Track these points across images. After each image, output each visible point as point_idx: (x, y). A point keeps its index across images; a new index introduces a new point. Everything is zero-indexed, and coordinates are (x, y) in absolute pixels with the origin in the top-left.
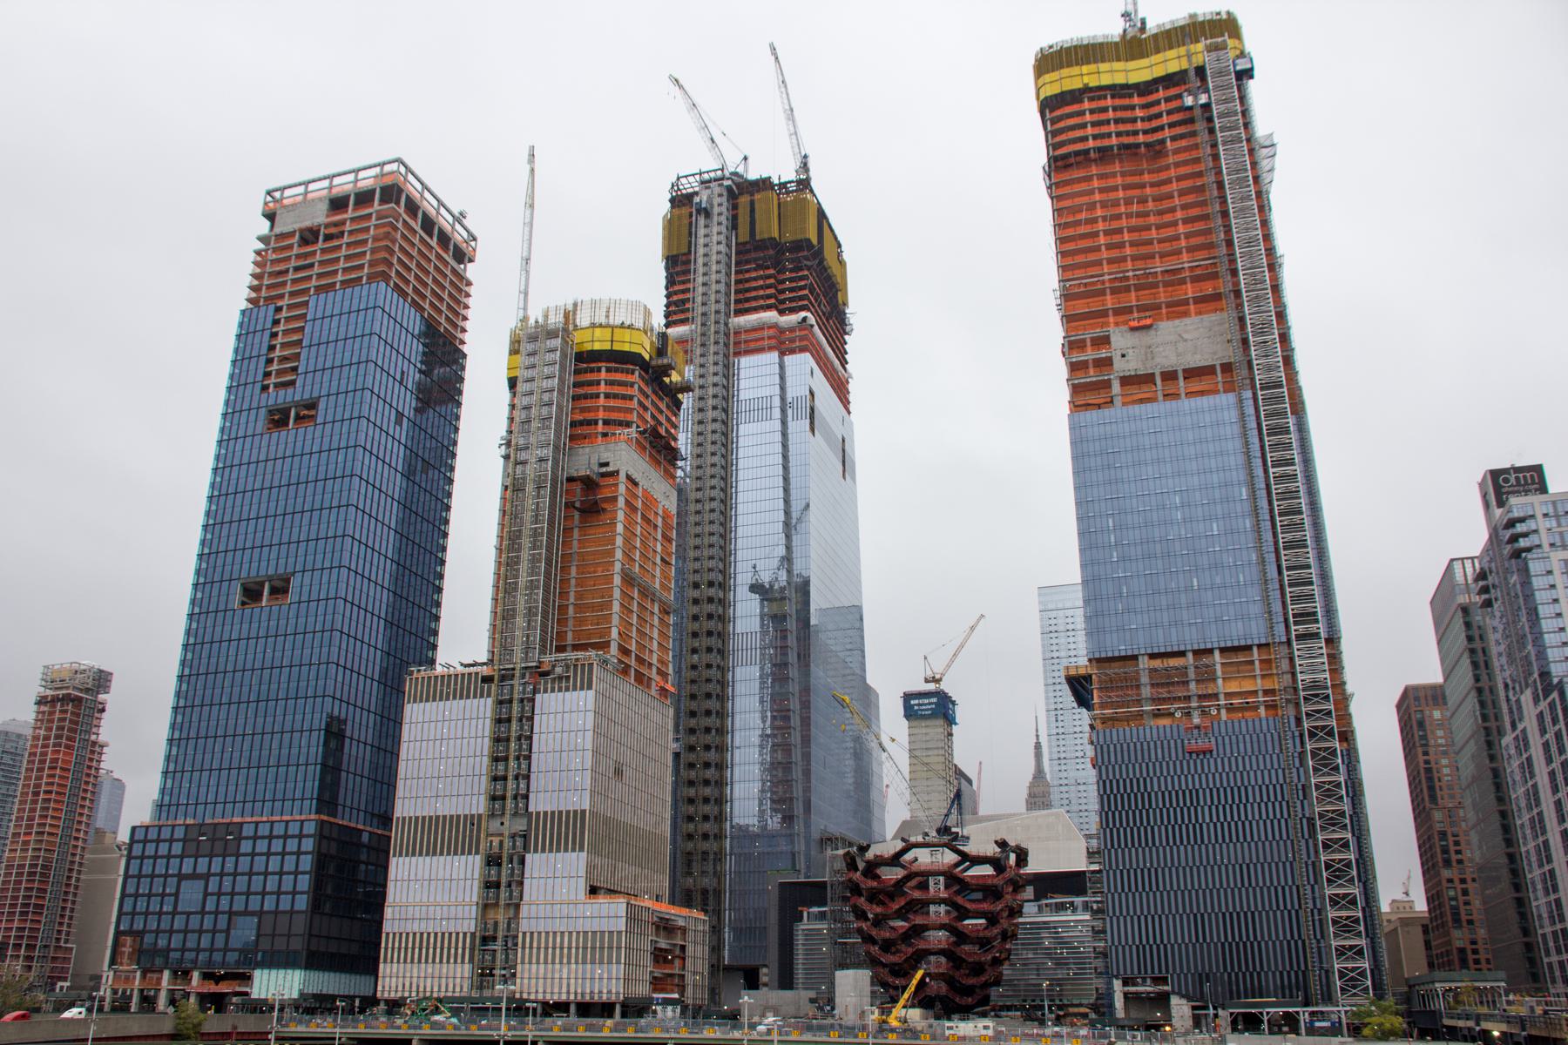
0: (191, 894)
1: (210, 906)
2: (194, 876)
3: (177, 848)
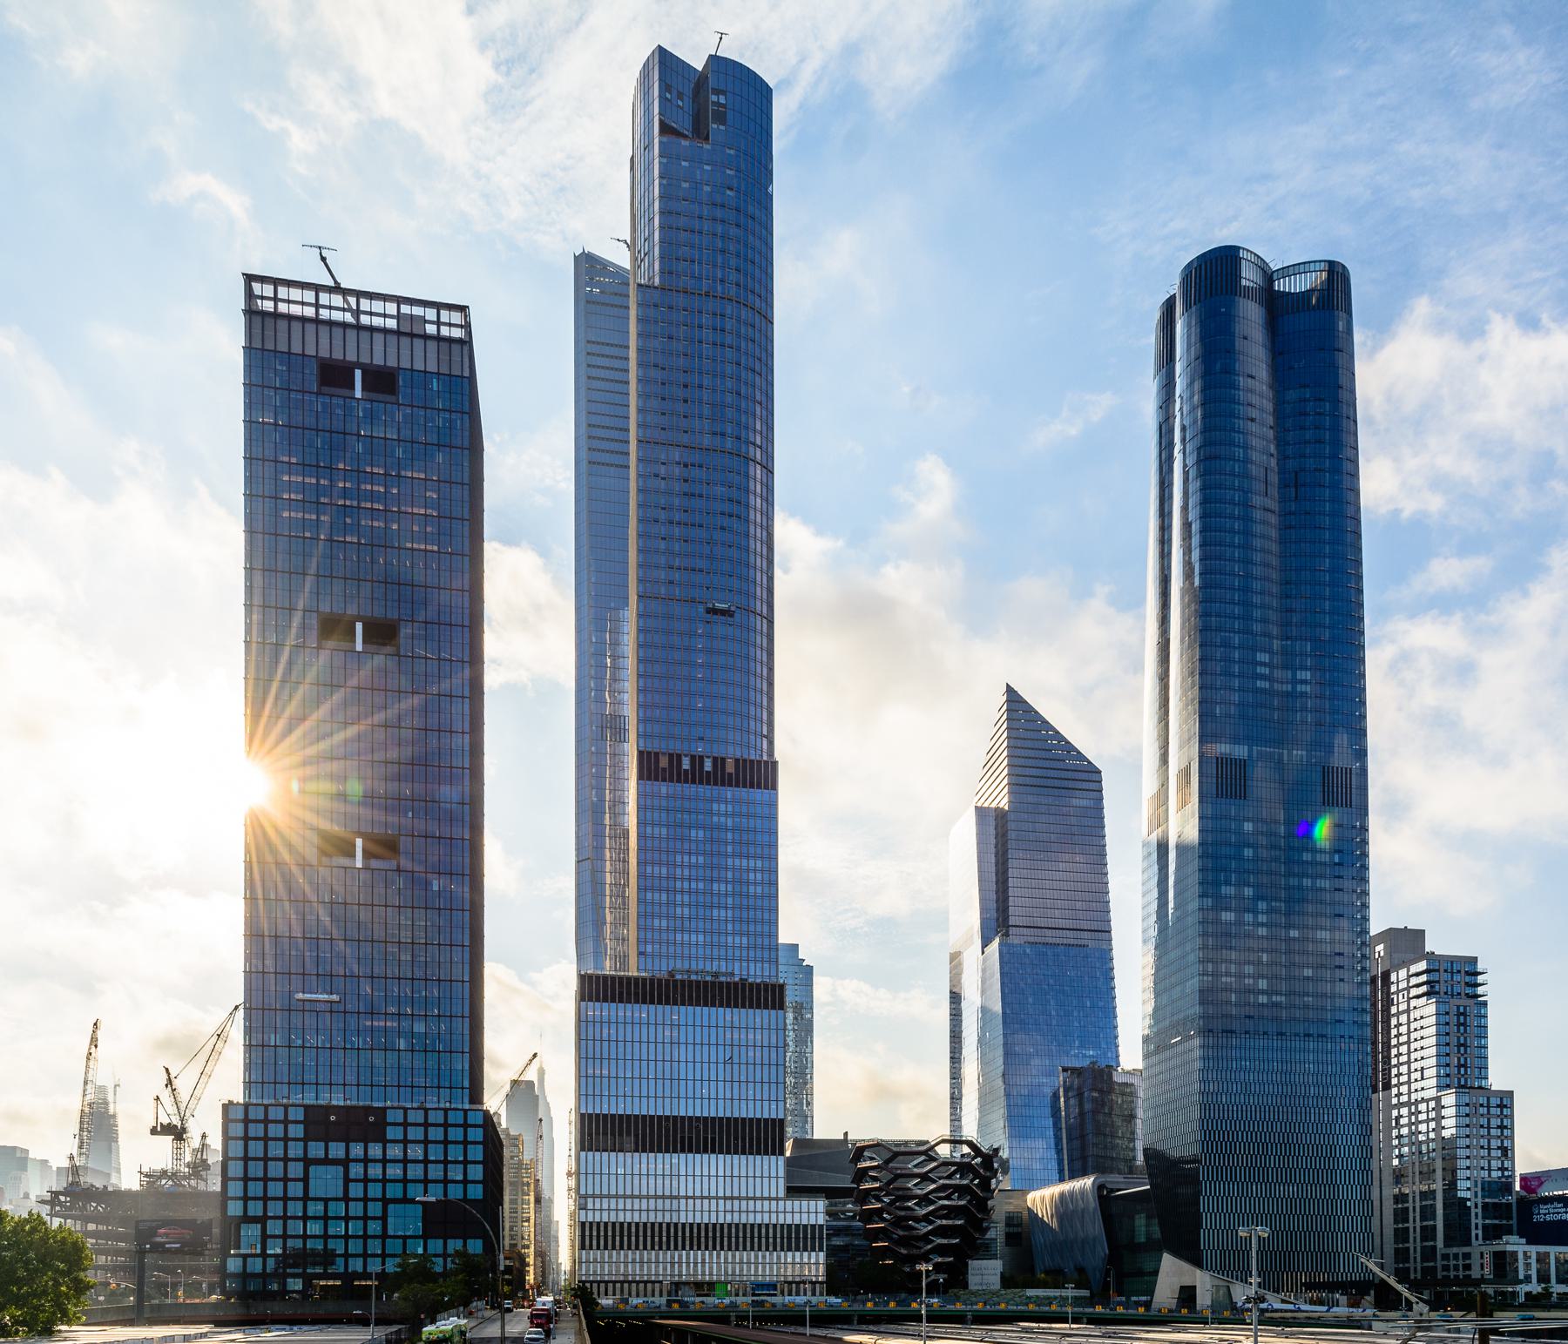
0: (326, 1181)
1: (356, 1190)
2: (326, 1161)
3: (297, 1131)
